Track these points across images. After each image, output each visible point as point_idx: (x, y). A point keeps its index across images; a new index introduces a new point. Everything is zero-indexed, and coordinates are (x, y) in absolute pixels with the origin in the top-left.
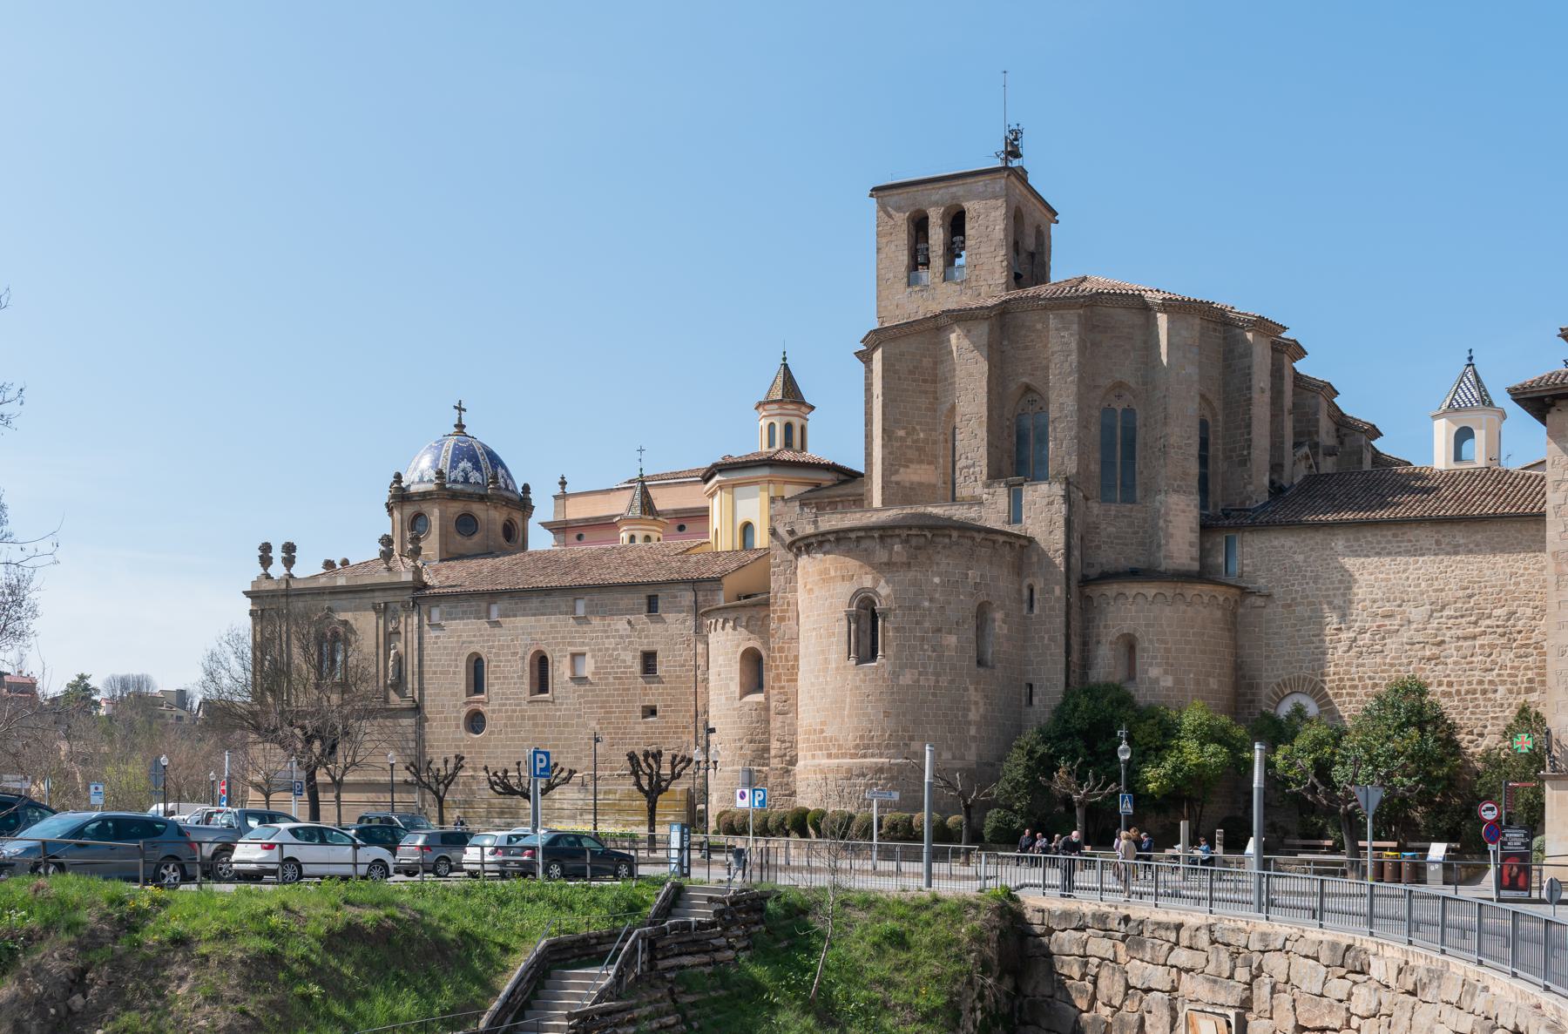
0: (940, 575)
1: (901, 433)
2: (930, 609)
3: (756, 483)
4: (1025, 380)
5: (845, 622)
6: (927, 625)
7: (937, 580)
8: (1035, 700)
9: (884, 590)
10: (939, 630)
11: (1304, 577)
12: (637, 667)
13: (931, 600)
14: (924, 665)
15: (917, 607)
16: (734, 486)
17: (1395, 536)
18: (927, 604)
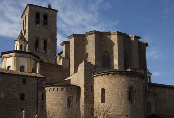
3: (26, 57)
9: (135, 87)
12: (19, 98)
16: (7, 58)
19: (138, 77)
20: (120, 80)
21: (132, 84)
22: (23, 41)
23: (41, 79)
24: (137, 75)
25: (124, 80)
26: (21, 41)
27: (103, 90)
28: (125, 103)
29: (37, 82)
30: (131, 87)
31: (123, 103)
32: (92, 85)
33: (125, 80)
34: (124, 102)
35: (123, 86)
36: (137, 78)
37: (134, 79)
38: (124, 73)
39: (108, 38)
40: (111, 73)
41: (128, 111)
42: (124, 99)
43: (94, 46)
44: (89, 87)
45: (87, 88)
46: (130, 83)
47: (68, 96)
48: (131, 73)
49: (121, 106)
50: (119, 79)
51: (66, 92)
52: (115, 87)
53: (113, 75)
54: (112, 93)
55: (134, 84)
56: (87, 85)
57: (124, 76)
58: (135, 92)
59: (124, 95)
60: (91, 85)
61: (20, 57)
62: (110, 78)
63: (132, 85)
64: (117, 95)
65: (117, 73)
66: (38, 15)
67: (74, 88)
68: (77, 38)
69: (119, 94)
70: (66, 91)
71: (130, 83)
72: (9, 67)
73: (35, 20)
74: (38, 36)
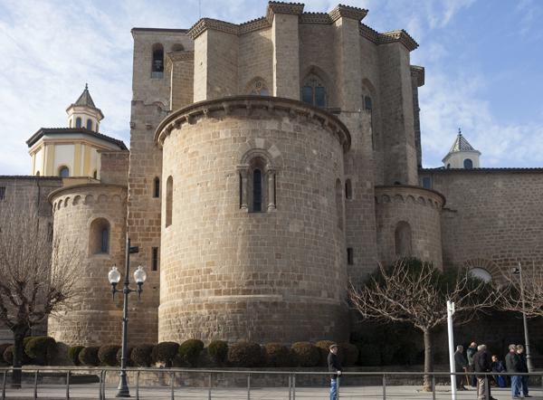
0: (317, 149)
1: (218, 89)
2: (311, 173)
3: (72, 143)
4: (312, 63)
5: (236, 177)
6: (309, 186)
7: (315, 152)
8: (355, 260)
9: (275, 152)
10: (316, 191)
11: (478, 201)
13: (312, 166)
14: (308, 218)
15: (302, 170)
17: (534, 180)
18: (308, 169)
19: (292, 117)
20: (214, 134)
21: (260, 143)
22: (82, 108)
23: (51, 184)
24: (288, 110)
25: (227, 134)
26: (76, 108)
27: (170, 180)
28: (228, 216)
29: (37, 191)
30: (256, 155)
31: (222, 216)
32: (158, 175)
33: (232, 132)
34: (223, 214)
35: (222, 155)
36: (286, 120)
37: (271, 125)
38: (225, 105)
39: (261, 38)
40: (183, 120)
41: (240, 243)
42: (226, 199)
43: (205, 66)
44: (145, 181)
45: (139, 186)
46: (252, 143)
47: (92, 219)
48: (251, 102)
49: (215, 229)
50: (210, 131)
51: (88, 206)
52: (197, 163)
53: (192, 120)
54: (189, 187)
55: (268, 145)
56: (140, 176)
57: (228, 120)
58: (275, 173)
59: (224, 186)
60: (154, 176)
61: (56, 144)
62: (184, 137)
63: (258, 146)
64: (202, 191)
65: (200, 114)
66: (158, 54)
67: (113, 194)
68: (182, 62)
69: (209, 185)
70: (86, 203)
71: (252, 143)
72: (38, 172)
73: (149, 64)
74: (157, 100)
